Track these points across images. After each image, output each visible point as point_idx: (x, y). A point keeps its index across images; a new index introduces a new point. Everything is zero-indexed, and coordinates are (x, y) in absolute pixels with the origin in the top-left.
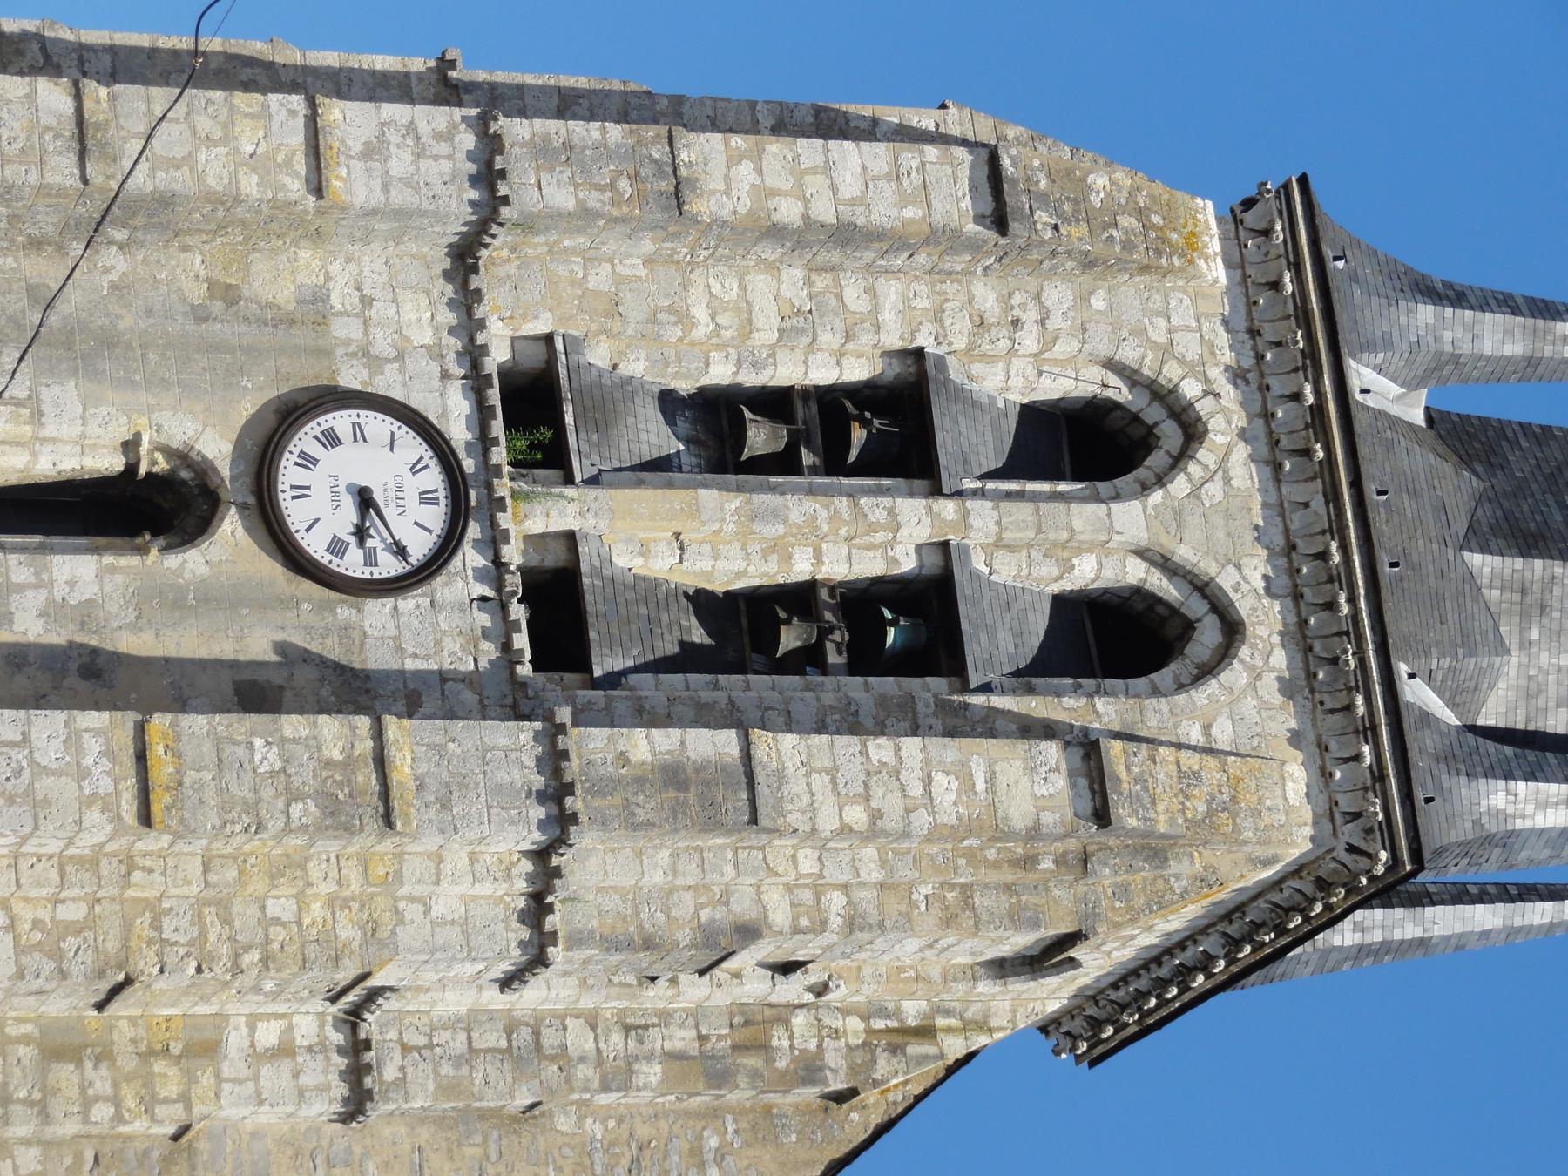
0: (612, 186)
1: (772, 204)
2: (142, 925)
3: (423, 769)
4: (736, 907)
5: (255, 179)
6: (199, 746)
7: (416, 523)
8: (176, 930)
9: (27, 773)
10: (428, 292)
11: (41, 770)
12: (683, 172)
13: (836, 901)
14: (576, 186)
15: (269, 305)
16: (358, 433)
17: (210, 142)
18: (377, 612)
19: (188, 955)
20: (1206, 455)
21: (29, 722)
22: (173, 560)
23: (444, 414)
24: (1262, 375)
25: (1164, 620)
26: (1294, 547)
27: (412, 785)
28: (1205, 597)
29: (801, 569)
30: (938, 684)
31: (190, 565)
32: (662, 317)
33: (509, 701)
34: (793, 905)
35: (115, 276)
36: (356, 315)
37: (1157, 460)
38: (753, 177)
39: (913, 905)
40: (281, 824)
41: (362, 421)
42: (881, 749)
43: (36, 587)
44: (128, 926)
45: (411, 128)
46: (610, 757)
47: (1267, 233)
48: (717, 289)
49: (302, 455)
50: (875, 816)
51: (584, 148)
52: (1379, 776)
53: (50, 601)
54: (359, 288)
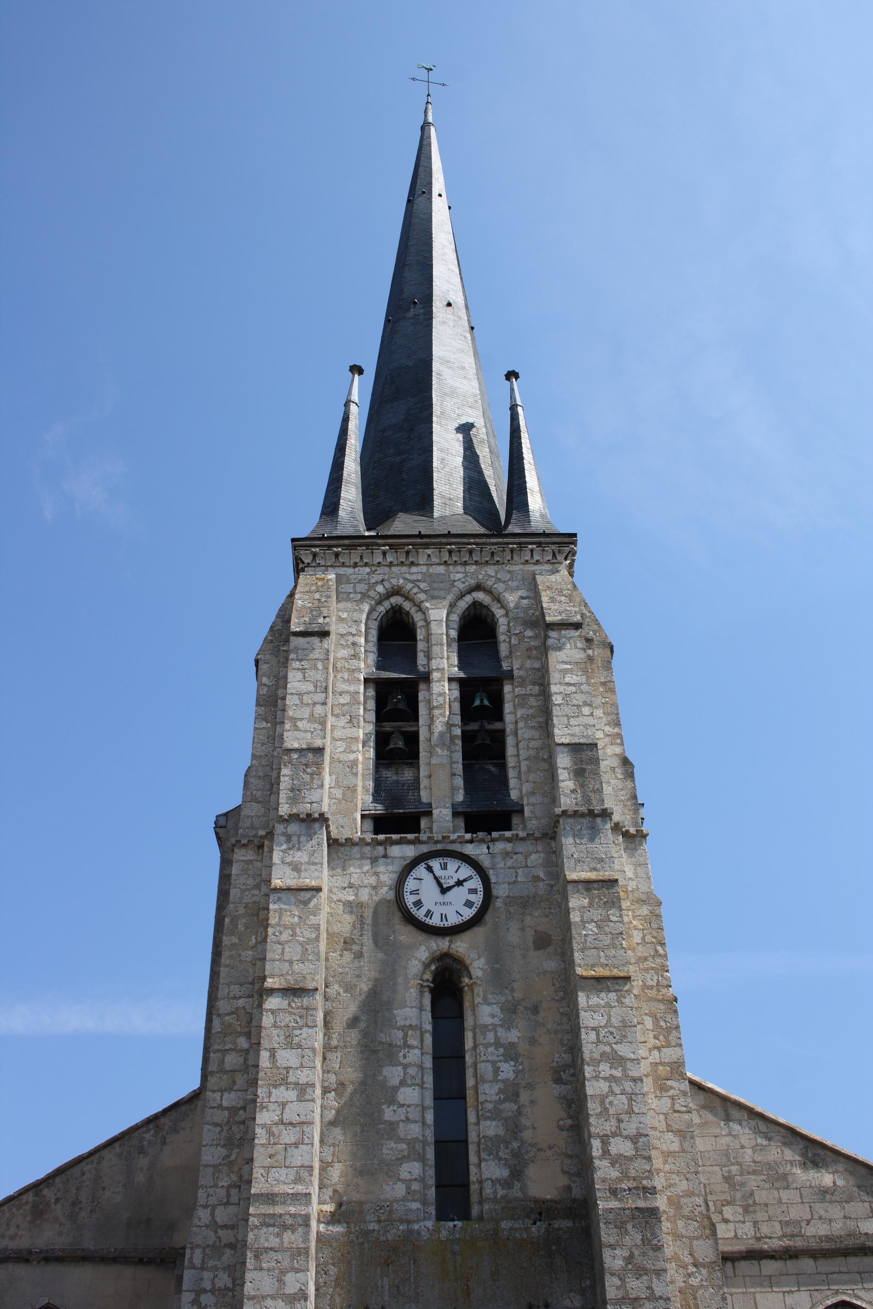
0: (312, 774)
1: (316, 716)
2: (652, 993)
3: (586, 868)
4: (615, 765)
5: (311, 917)
6: (588, 956)
7: (454, 870)
8: (652, 980)
9: (611, 1029)
10: (345, 861)
12: (304, 746)
13: (607, 729)
14: (311, 788)
15: (354, 926)
16: (415, 892)
17: (294, 935)
19: (662, 976)
21: (587, 1027)
23: (404, 858)
24: (373, 565)
25: (469, 614)
26: (446, 562)
27: (595, 873)
28: (464, 595)
29: (458, 732)
30: (507, 688)
31: (481, 966)
32: (354, 771)
33: (534, 842)
34: (612, 744)
35: (341, 991)
36: (358, 890)
37: (407, 606)
39: (607, 703)
40: (621, 925)
41: (409, 891)
42: (557, 699)
43: (496, 1032)
44: (651, 999)
46: (573, 796)
47: (315, 555)
48: (341, 749)
49: (426, 915)
50: (585, 704)
51: (293, 784)
52: (539, 544)
53: (501, 1026)
54: (345, 888)
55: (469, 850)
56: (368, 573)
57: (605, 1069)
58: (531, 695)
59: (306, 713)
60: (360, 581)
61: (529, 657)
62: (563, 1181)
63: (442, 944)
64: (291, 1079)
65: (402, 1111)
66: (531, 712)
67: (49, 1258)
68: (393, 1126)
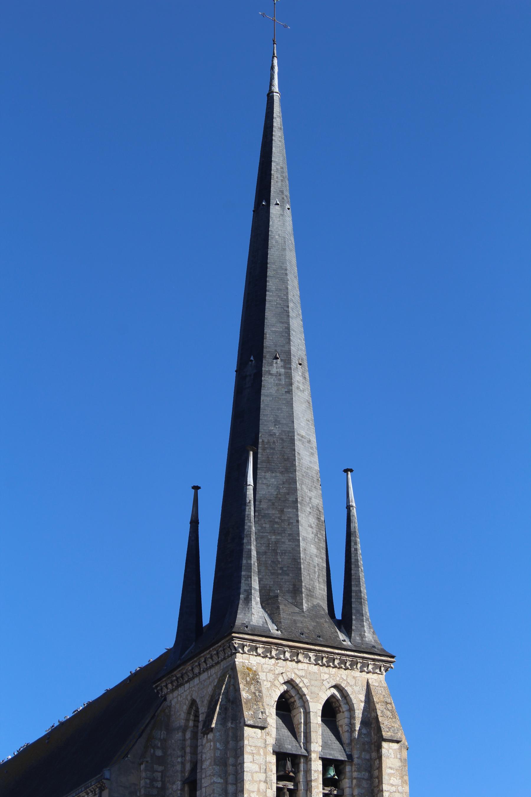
20: (298, 681)
37: (293, 693)
38: (255, 794)
56: (274, 665)
58: (363, 779)
59: (256, 789)
61: (364, 750)
66: (363, 791)
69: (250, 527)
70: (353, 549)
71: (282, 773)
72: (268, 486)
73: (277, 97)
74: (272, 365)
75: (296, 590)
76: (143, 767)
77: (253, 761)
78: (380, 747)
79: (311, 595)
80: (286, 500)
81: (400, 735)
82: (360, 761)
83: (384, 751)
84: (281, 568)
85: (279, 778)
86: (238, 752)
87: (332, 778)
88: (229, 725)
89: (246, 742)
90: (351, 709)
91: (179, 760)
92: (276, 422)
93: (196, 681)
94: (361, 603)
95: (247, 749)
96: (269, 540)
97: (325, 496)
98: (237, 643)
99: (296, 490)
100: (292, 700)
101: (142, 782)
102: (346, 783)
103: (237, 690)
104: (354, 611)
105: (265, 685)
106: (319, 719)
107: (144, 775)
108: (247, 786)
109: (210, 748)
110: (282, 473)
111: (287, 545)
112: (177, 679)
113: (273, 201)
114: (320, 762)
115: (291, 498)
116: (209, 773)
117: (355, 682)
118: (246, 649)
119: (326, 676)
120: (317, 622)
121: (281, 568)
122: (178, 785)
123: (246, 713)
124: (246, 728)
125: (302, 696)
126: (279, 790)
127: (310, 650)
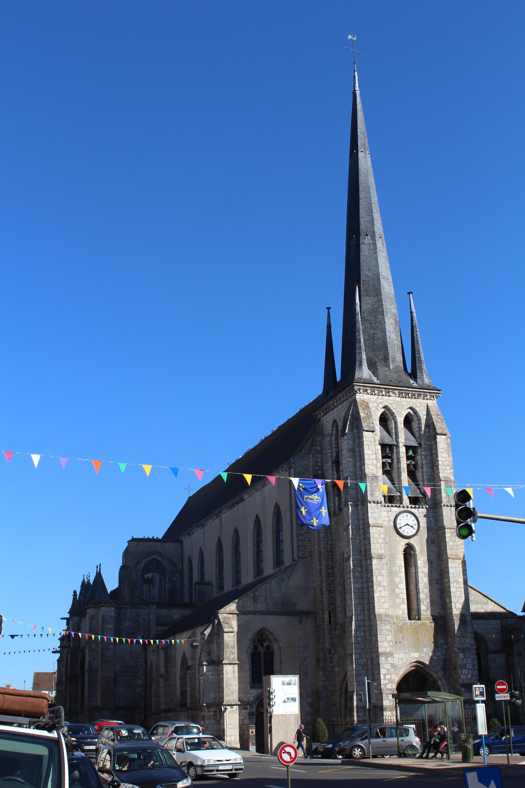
11: (456, 572)
17: (377, 541)
18: (421, 525)
20: (390, 406)
22: (417, 551)
37: (388, 412)
45: (372, 513)
55: (413, 510)
57: (455, 584)
59: (371, 463)
60: (375, 402)
62: (439, 611)
63: (407, 541)
64: (382, 584)
65: (400, 590)
66: (428, 462)
67: (262, 613)
68: (398, 595)
69: (359, 326)
70: (415, 335)
71: (384, 454)
72: (367, 304)
73: (358, 93)
74: (365, 239)
75: (386, 359)
76: (310, 456)
77: (369, 449)
78: (435, 438)
79: (394, 360)
80: (377, 311)
81: (446, 431)
82: (425, 446)
83: (438, 440)
84: (377, 347)
85: (383, 457)
86: (361, 445)
87: (411, 456)
88: (355, 431)
89: (364, 439)
90: (419, 419)
91: (330, 451)
92: (370, 270)
93: (336, 410)
94: (421, 363)
95: (365, 443)
96: (369, 333)
97: (398, 308)
98: (356, 388)
99: (382, 305)
100: (387, 416)
101: (311, 464)
102: (418, 458)
103: (358, 413)
104: (417, 368)
105: (373, 409)
106: (403, 425)
107: (311, 460)
108: (366, 462)
109: (345, 443)
110: (374, 297)
111: (380, 335)
112: (326, 409)
113: (360, 150)
114: (404, 448)
115: (380, 310)
116: (346, 456)
117: (420, 405)
118: (361, 391)
119: (405, 403)
120: (398, 375)
121: (377, 347)
122: (330, 464)
123: (363, 424)
124: (364, 432)
125: (392, 414)
126: (383, 463)
127: (396, 389)
